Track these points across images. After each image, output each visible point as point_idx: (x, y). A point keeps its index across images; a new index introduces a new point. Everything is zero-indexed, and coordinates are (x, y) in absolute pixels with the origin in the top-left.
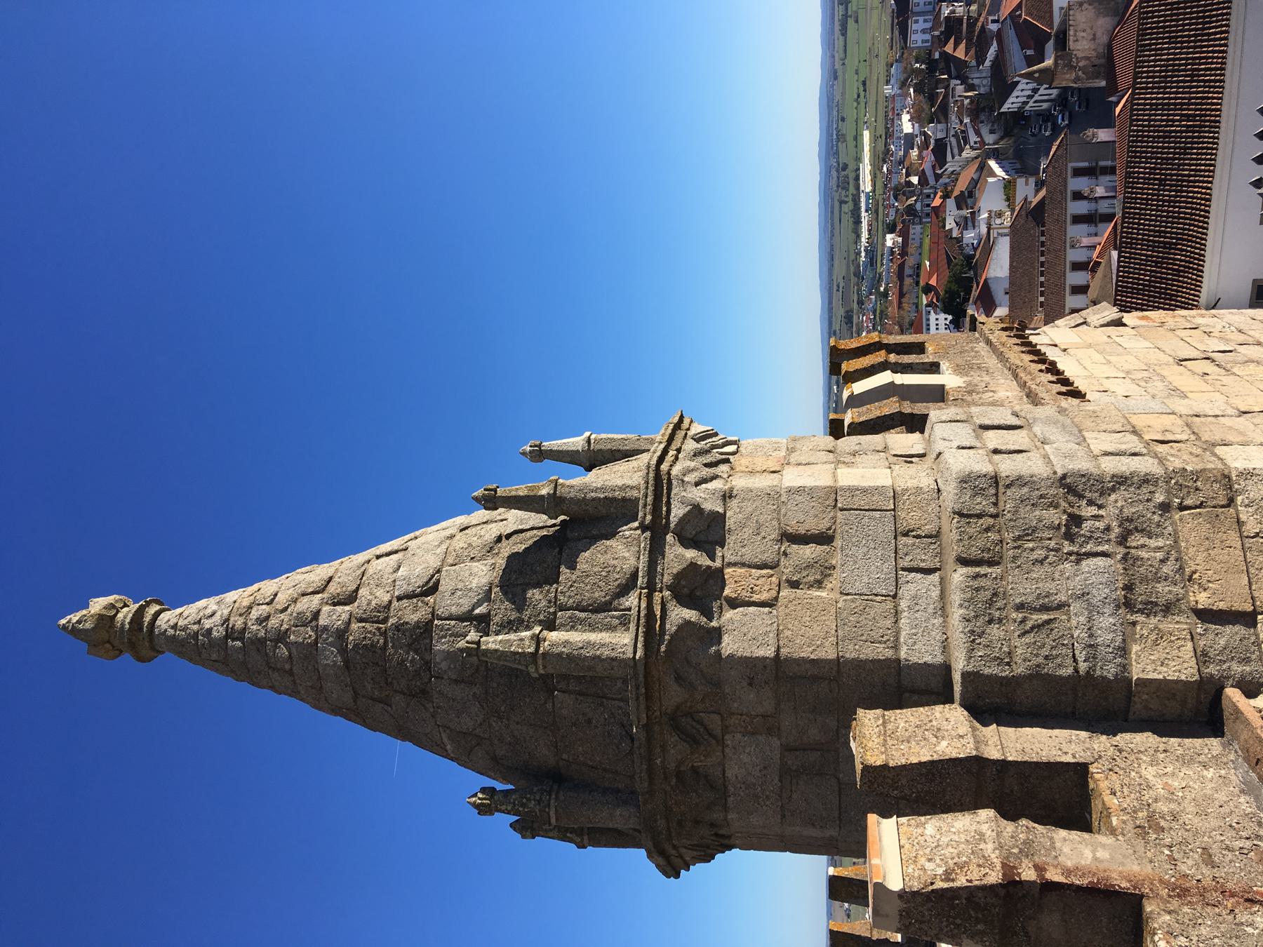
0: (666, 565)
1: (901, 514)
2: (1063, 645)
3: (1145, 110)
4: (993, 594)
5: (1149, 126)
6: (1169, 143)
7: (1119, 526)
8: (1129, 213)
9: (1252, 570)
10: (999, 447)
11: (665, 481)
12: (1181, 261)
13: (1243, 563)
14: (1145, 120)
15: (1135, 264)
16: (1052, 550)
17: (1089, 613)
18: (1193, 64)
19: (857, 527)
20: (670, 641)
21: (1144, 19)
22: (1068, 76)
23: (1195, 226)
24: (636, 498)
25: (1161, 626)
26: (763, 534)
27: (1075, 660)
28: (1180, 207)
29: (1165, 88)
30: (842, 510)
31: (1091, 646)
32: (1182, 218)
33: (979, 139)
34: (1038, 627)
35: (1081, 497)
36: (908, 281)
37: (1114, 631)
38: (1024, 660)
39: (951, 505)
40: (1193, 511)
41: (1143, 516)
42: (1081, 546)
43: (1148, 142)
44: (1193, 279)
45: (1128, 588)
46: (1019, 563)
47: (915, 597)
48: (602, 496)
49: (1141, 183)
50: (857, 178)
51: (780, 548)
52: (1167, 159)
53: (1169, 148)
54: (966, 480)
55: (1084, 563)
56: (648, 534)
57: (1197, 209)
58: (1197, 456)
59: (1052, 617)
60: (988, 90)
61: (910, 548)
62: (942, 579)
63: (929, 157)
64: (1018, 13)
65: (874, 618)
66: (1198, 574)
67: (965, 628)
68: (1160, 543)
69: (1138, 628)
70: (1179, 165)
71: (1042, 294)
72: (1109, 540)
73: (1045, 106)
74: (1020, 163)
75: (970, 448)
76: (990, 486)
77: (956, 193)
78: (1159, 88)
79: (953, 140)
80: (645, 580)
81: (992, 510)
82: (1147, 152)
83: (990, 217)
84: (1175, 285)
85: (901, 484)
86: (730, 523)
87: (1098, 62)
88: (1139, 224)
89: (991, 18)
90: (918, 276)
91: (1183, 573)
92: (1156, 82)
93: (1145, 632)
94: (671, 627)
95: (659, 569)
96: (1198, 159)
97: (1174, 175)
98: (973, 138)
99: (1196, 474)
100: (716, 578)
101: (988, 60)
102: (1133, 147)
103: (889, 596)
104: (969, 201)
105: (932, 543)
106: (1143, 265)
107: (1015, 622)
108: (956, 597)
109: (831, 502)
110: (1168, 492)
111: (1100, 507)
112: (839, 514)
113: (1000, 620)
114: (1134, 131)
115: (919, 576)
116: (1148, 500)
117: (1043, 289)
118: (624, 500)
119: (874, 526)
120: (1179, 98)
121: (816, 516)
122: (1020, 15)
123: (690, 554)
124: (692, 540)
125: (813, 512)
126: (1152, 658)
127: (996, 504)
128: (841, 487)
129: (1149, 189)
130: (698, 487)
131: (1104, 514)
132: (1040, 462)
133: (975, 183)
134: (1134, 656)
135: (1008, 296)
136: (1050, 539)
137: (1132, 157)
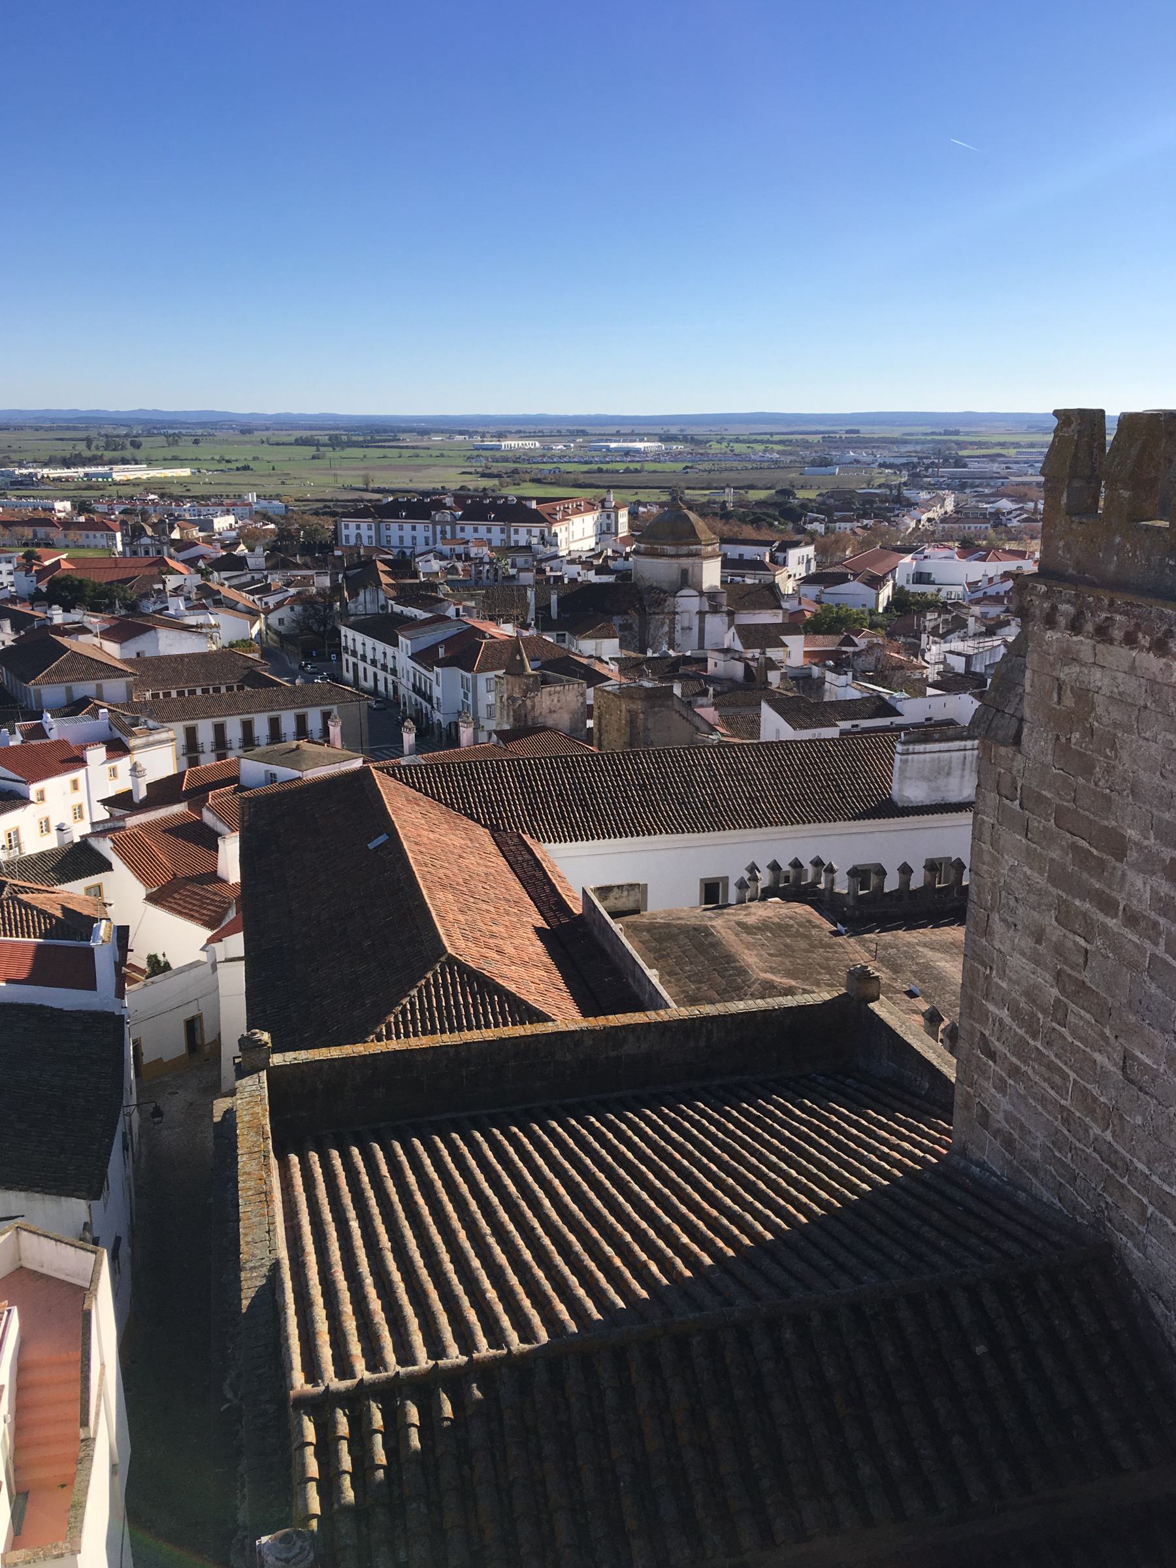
3: (703, 759)
5: (690, 765)
8: (598, 760)
12: (575, 817)
14: (694, 762)
15: (550, 774)
28: (627, 808)
32: (617, 811)
36: (28, 532)
44: (563, 832)
49: (633, 767)
50: (125, 461)
52: (667, 788)
53: (678, 788)
60: (351, 612)
70: (666, 800)
73: (349, 676)
79: (248, 577)
82: (665, 768)
83: (210, 626)
84: (546, 816)
89: (461, 607)
90: (38, 545)
96: (679, 816)
98: (272, 601)
101: (402, 608)
114: (679, 752)
117: (161, 697)
122: (485, 638)
129: (631, 775)
135: (134, 656)
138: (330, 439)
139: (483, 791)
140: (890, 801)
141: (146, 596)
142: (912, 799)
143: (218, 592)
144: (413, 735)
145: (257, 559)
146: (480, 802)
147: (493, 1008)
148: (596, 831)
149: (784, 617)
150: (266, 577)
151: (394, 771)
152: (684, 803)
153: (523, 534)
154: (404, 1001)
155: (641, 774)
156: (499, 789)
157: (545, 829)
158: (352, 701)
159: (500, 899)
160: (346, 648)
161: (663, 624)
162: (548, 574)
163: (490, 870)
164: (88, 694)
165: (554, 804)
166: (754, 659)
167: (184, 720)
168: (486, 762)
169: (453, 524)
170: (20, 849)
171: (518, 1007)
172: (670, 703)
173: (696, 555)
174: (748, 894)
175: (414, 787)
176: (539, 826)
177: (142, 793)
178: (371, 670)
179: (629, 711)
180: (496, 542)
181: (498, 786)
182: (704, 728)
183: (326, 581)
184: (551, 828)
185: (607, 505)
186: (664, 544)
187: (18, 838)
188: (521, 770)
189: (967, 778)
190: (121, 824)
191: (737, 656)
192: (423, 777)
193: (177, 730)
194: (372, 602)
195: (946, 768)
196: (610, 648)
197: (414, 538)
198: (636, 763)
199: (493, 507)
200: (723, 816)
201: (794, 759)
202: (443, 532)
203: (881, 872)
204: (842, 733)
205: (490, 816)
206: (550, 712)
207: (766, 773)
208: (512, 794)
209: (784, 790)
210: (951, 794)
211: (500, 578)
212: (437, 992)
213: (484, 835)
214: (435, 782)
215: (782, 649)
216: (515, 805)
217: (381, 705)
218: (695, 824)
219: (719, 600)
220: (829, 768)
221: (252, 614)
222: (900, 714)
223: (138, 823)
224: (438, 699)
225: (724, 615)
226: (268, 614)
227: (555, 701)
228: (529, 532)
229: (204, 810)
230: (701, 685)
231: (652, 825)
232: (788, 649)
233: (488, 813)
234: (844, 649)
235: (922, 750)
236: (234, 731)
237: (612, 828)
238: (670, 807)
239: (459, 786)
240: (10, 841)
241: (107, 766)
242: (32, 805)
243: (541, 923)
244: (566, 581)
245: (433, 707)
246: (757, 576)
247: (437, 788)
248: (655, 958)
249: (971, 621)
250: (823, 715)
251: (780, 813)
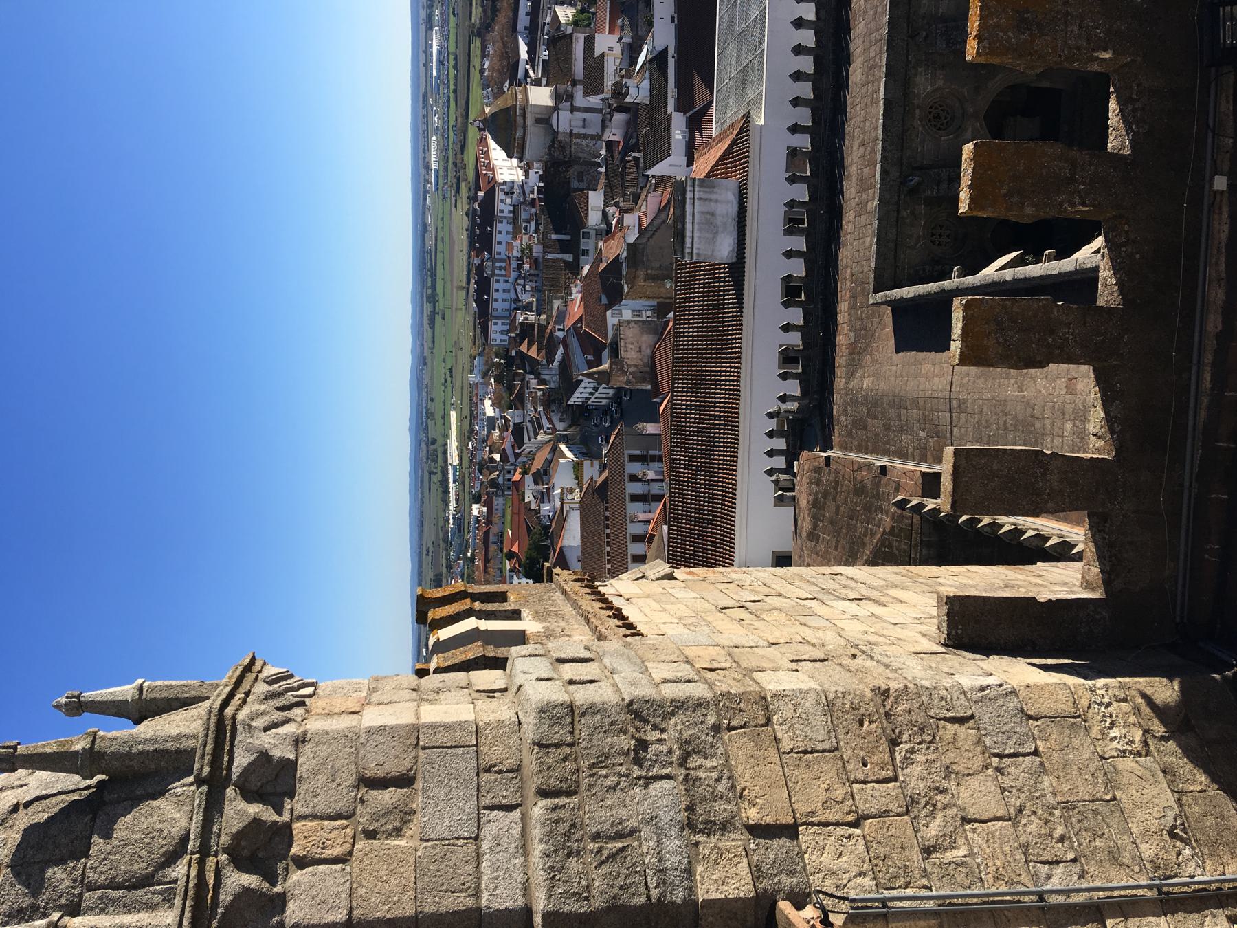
0: (224, 824)
1: (484, 749)
2: (636, 872)
4: (572, 825)
6: (702, 437)
7: (679, 749)
8: (676, 493)
9: (790, 784)
10: (574, 678)
11: (229, 727)
12: (718, 534)
13: (783, 778)
15: (682, 536)
16: (623, 776)
17: (658, 837)
18: (716, 376)
19: (439, 765)
20: (223, 915)
21: (677, 337)
22: (621, 379)
23: (726, 505)
24: (192, 748)
25: (720, 845)
26: (338, 780)
27: (648, 888)
28: (713, 490)
30: (424, 748)
31: (661, 871)
33: (551, 426)
34: (612, 856)
35: (646, 722)
36: (493, 548)
37: (680, 854)
38: (601, 893)
39: (531, 736)
40: (739, 731)
41: (699, 738)
42: (648, 770)
44: (727, 550)
45: (690, 808)
46: (594, 791)
47: (497, 837)
48: (151, 748)
49: (682, 468)
50: (445, 452)
51: (356, 795)
54: (545, 710)
55: (651, 787)
56: (204, 788)
57: (726, 492)
58: (739, 681)
59: (625, 844)
61: (492, 784)
62: (523, 814)
63: (509, 438)
64: (579, 325)
65: (455, 864)
66: (747, 791)
67: (545, 864)
68: (714, 762)
69: (701, 848)
70: (711, 455)
72: (672, 763)
73: (604, 402)
74: (587, 449)
75: (548, 680)
76: (567, 715)
77: (533, 470)
78: (692, 392)
80: (198, 843)
81: (569, 739)
82: (686, 444)
83: (562, 493)
85: (484, 718)
86: (302, 770)
89: (557, 327)
90: (502, 543)
91: (735, 791)
92: (689, 388)
93: (707, 852)
94: (225, 897)
95: (215, 829)
96: (724, 451)
97: (707, 463)
98: (546, 424)
99: (740, 698)
100: (284, 833)
101: (556, 361)
102: (674, 438)
103: (470, 838)
104: (545, 478)
105: (513, 778)
106: (688, 537)
107: (592, 852)
108: (536, 832)
109: (412, 741)
110: (718, 714)
111: (663, 731)
112: (421, 753)
113: (578, 852)
114: (675, 425)
115: (501, 813)
116: (702, 723)
118: (178, 751)
119: (457, 763)
120: (708, 402)
121: (396, 757)
122: (581, 327)
123: (254, 809)
124: (257, 792)
125: (393, 752)
126: (714, 877)
127: (572, 733)
128: (423, 724)
129: (689, 474)
130: (267, 733)
131: (666, 737)
132: (610, 690)
133: (549, 463)
134: (698, 877)
136: (621, 765)
137: (674, 447)
142: (731, 248)
144: (648, 425)
148: (728, 524)
149: (579, 32)
153: (504, 206)
155: (689, 465)
158: (622, 439)
162: (535, 196)
167: (627, 563)
169: (495, 261)
172: (641, 247)
173: (524, 109)
180: (510, 228)
182: (663, 216)
186: (515, 138)
191: (609, 116)
195: (708, 217)
196: (596, 199)
197: (504, 291)
199: (482, 227)
202: (501, 268)
203: (791, 204)
204: (678, 109)
206: (640, 351)
207: (697, 362)
210: (730, 211)
211: (536, 272)
215: (605, 58)
219: (562, 91)
222: (666, 50)
225: (575, 88)
226: (556, 429)
228: (503, 201)
230: (630, 161)
232: (606, 52)
235: (691, 240)
238: (717, 455)
244: (542, 184)
246: (545, 8)
250: (661, 123)
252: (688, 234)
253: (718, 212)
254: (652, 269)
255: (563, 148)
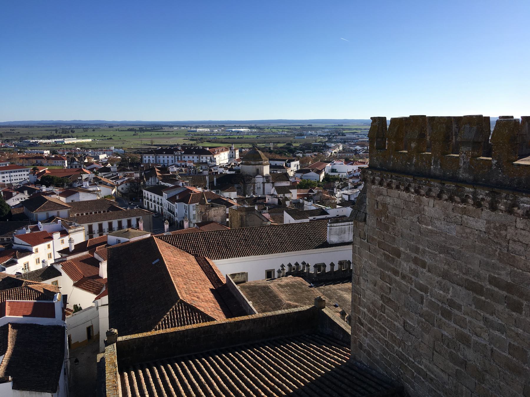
3: (265, 230)
5: (261, 233)
6: (259, 240)
8: (230, 232)
12: (223, 251)
15: (214, 237)
22: (203, 209)
28: (240, 247)
29: (275, 235)
36: (34, 161)
43: (256, 233)
50: (69, 137)
52: (254, 240)
53: (257, 240)
60: (147, 185)
70: (253, 244)
71: (87, 214)
73: (146, 206)
83: (98, 191)
87: (207, 218)
88: (228, 235)
89: (184, 183)
90: (38, 165)
98: (119, 182)
101: (164, 183)
106: (215, 239)
114: (257, 228)
117: (80, 215)
135: (71, 202)
138: (140, 129)
139: (192, 243)
140: (326, 242)
141: (75, 181)
143: (101, 179)
145: (114, 168)
146: (191, 247)
147: (196, 318)
148: (230, 255)
150: (117, 174)
151: (161, 237)
152: (259, 245)
154: (165, 317)
155: (245, 236)
156: (197, 242)
157: (213, 255)
158: (147, 215)
159: (198, 279)
160: (145, 197)
161: (251, 187)
162: (213, 171)
163: (194, 270)
164: (54, 215)
165: (216, 247)
166: (281, 197)
168: (193, 233)
170: (29, 269)
171: (205, 317)
173: (262, 164)
174: (281, 275)
175: (168, 243)
176: (211, 254)
177: (73, 248)
178: (153, 204)
179: (240, 215)
180: (196, 161)
181: (197, 241)
182: (265, 220)
183: (138, 175)
184: (215, 255)
185: (232, 149)
187: (28, 266)
188: (205, 236)
189: (350, 234)
190: (65, 259)
191: (276, 197)
192: (171, 239)
193: (85, 226)
194: (154, 181)
196: (234, 195)
197: (168, 160)
198: (243, 232)
199: (194, 150)
200: (272, 249)
201: (295, 229)
202: (178, 158)
203: (324, 266)
205: (194, 252)
207: (286, 234)
208: (202, 244)
209: (292, 240)
212: (176, 313)
213: (192, 258)
214: (176, 241)
216: (203, 247)
217: (157, 216)
218: (263, 252)
220: (306, 232)
221: (112, 186)
222: (328, 214)
223: (71, 258)
224: (176, 213)
227: (216, 213)
228: (206, 158)
229: (95, 253)
230: (264, 206)
231: (249, 253)
232: (292, 194)
233: (194, 250)
234: (310, 193)
236: (105, 226)
237: (236, 254)
239: (184, 242)
240: (25, 267)
241: (60, 239)
242: (34, 254)
243: (212, 287)
244: (219, 173)
245: (175, 216)
247: (176, 243)
248: (251, 298)
249: (349, 184)
250: (304, 215)
251: (291, 247)
252: (338, 224)
253: (345, 235)
254: (246, 218)
255: (250, 180)
